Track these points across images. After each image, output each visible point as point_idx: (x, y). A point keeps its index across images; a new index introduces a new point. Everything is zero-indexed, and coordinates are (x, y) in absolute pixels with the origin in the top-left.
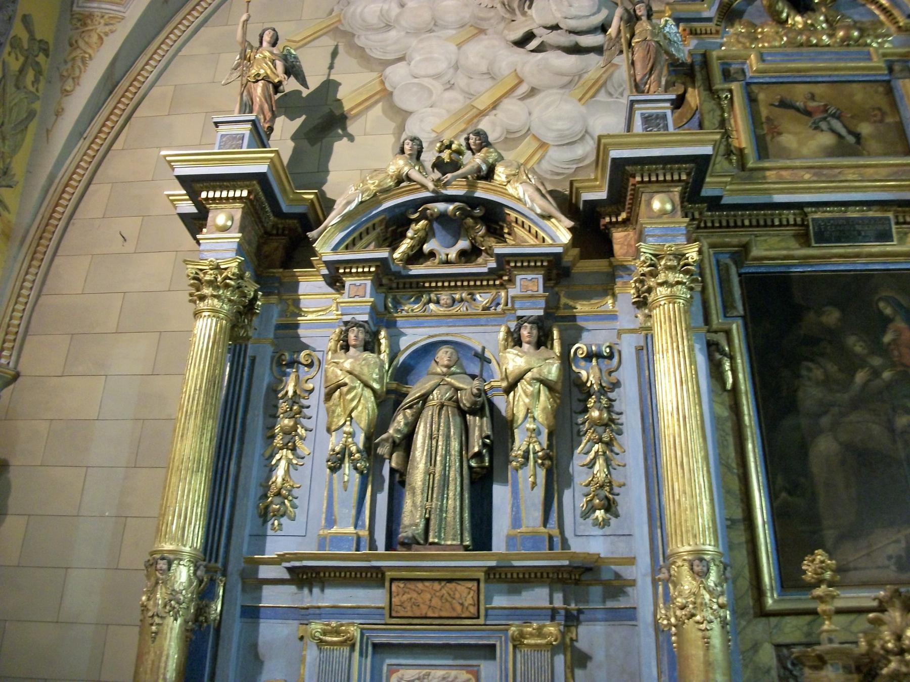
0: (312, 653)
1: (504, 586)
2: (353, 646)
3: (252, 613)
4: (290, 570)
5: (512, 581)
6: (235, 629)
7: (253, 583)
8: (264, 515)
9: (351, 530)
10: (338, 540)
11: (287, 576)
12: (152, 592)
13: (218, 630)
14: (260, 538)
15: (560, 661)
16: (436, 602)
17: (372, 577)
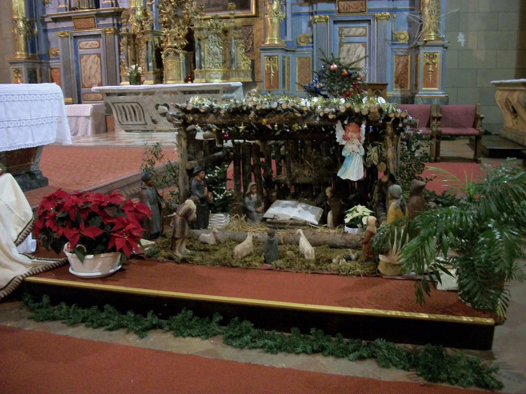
0: (60, 39)
1: (101, 18)
2: (68, 37)
3: (46, 31)
4: (52, 18)
5: (103, 17)
6: (42, 35)
7: (44, 23)
8: (44, 4)
9: (64, 6)
10: (61, 9)
11: (51, 20)
12: (14, 30)
13: (37, 36)
14: (44, 10)
15: (116, 37)
16: (85, 24)
17: (68, 19)
